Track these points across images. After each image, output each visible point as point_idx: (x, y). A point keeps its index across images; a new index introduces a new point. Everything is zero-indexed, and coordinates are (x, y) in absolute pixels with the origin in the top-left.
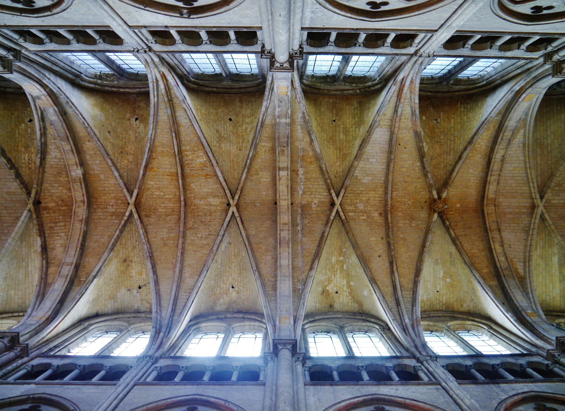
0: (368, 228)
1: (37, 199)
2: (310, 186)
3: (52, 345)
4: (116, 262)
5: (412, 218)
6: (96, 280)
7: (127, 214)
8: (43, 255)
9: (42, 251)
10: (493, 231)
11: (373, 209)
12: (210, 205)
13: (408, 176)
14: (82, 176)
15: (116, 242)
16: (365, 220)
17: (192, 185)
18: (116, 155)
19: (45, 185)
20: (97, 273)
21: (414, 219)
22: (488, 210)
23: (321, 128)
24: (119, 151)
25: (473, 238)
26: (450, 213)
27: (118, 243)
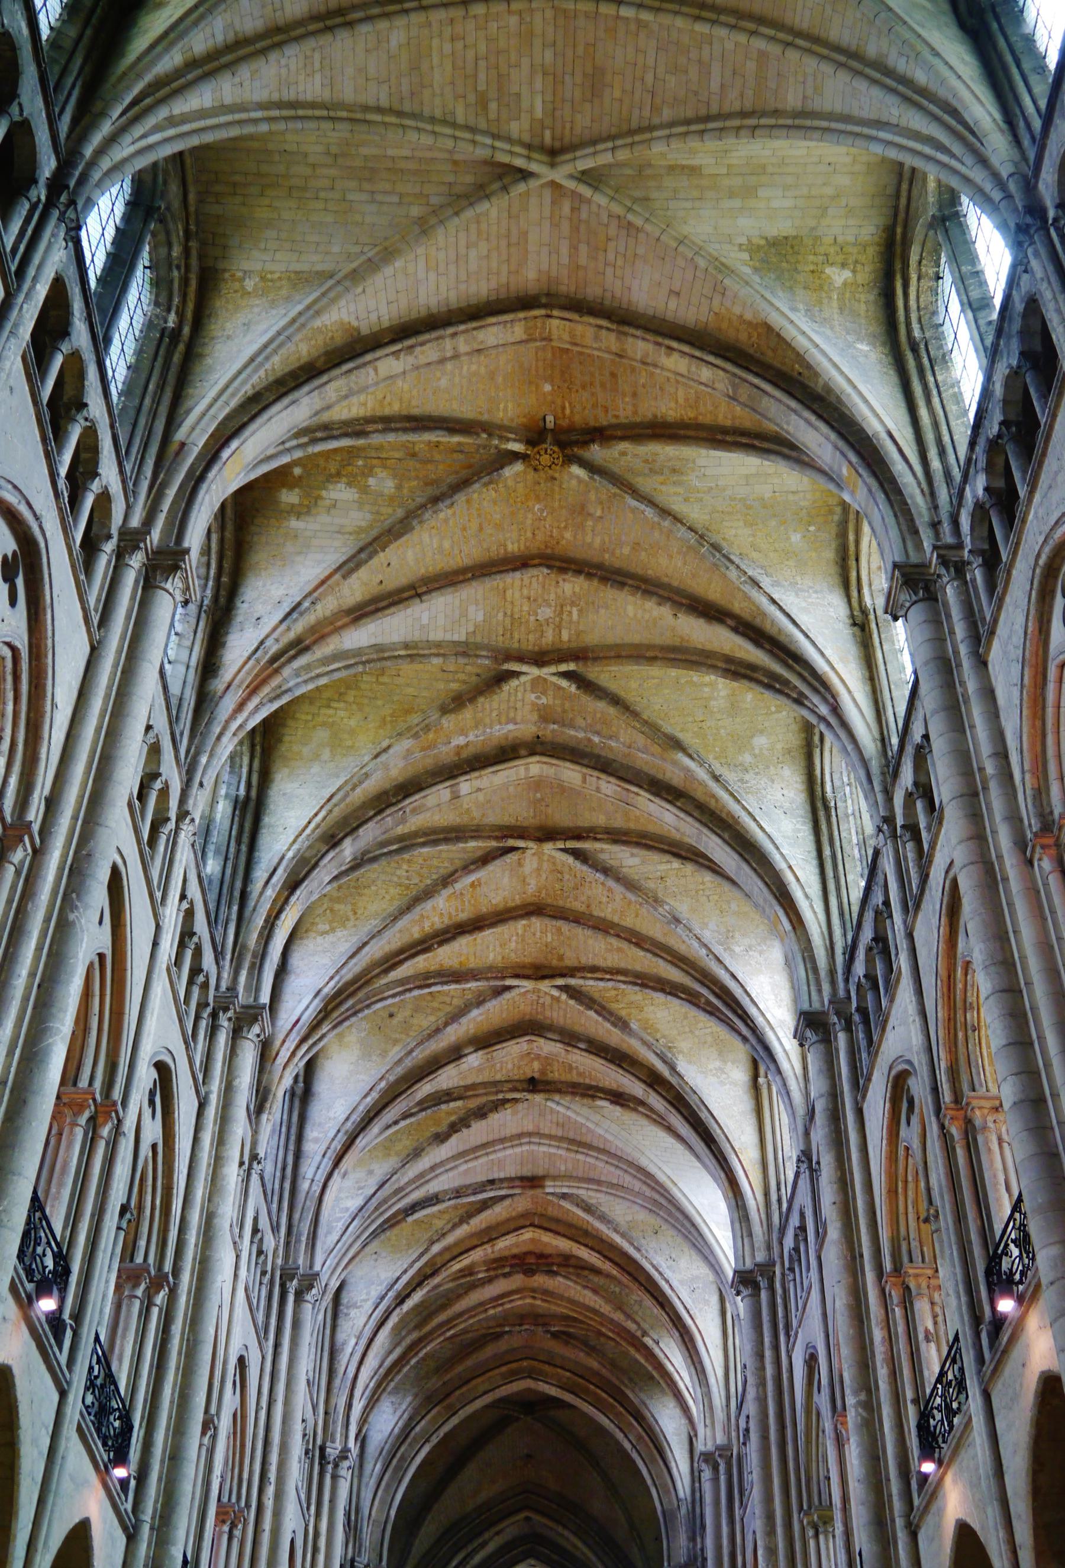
0: (602, 611)
1: (525, 1086)
2: (494, 714)
3: (774, 1197)
4: (652, 1008)
5: (581, 510)
6: (682, 1067)
7: (555, 993)
8: (628, 1107)
9: (622, 1105)
10: (623, 350)
11: (553, 589)
12: (538, 870)
13: (464, 529)
14: (480, 1053)
15: (611, 1013)
16: (580, 611)
17: (494, 902)
18: (435, 1004)
19: (498, 1077)
20: (665, 1062)
21: (583, 507)
22: (560, 339)
23: (348, 688)
24: (429, 998)
25: (642, 381)
26: (568, 412)
27: (614, 1006)
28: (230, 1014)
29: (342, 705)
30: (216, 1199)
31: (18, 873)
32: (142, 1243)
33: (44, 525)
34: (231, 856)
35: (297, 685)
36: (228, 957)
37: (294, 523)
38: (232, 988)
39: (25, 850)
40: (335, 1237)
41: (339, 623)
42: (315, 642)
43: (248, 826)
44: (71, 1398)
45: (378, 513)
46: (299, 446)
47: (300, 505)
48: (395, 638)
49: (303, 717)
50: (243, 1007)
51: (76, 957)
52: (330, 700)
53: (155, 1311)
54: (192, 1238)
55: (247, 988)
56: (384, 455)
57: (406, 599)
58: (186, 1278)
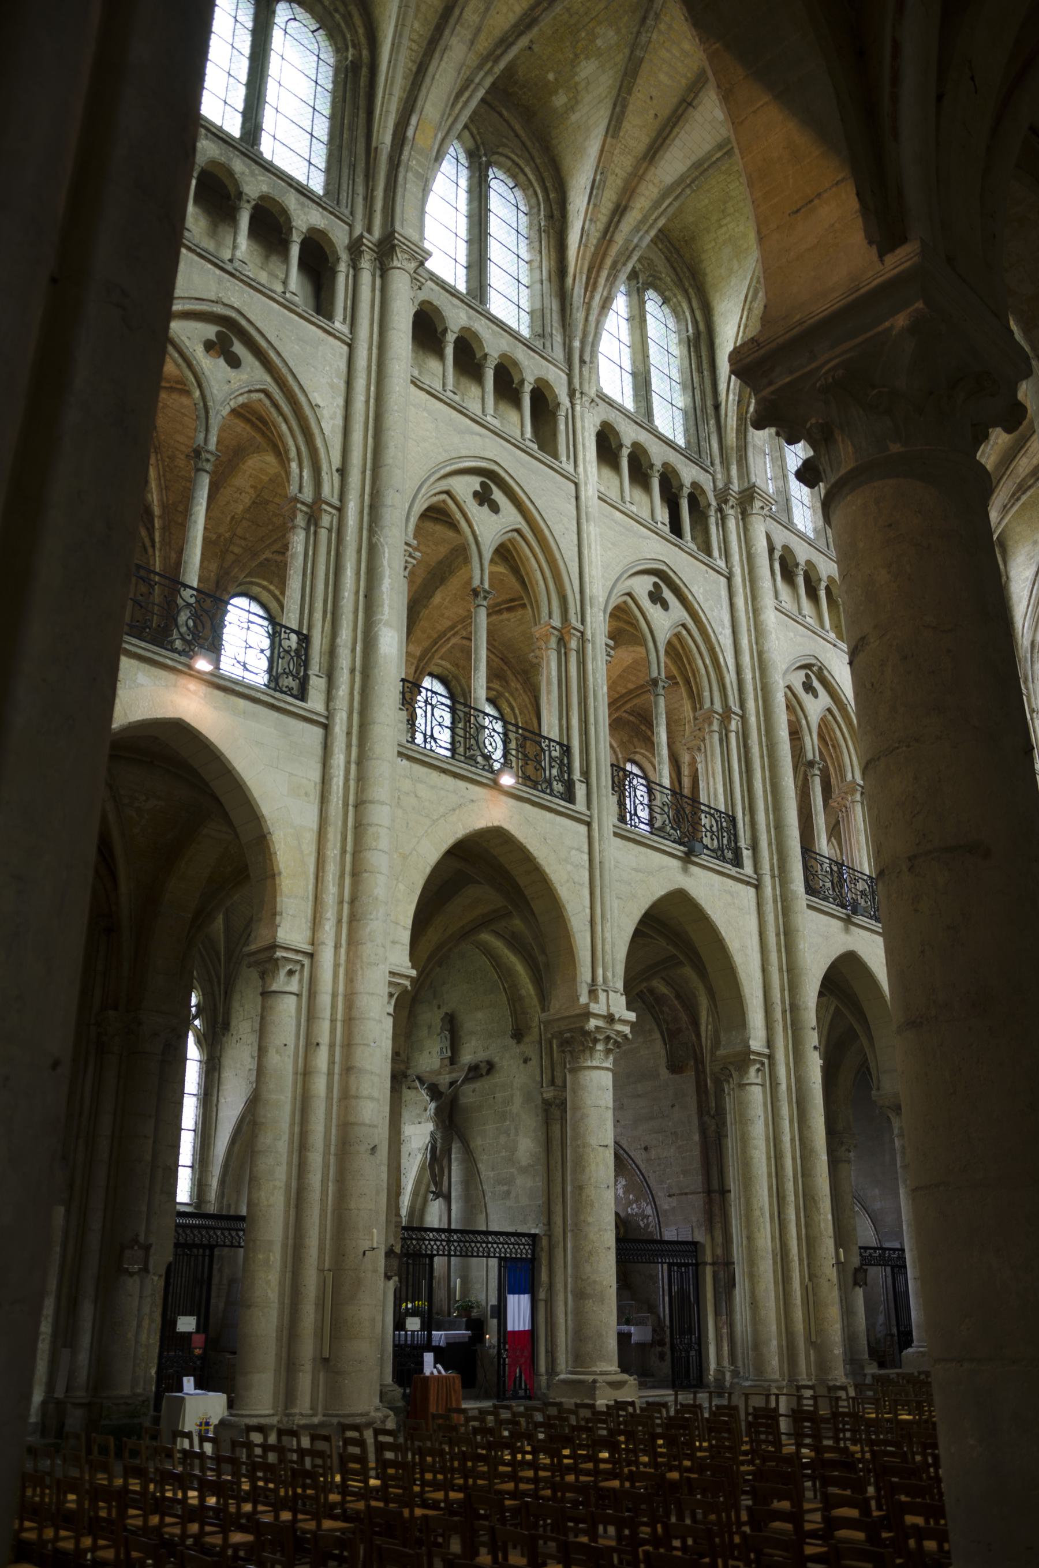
28: (732, 501)
29: (728, 219)
30: (760, 641)
31: (330, 531)
32: (706, 694)
33: (226, 301)
34: (696, 385)
35: (641, 239)
36: (717, 461)
37: (574, 118)
38: (729, 481)
39: (330, 513)
40: (1025, 603)
41: (641, 172)
42: (629, 200)
43: (704, 353)
44: (595, 826)
45: (616, 64)
46: (487, 74)
47: (570, 100)
48: (707, 147)
49: (710, 246)
50: (740, 493)
51: (382, 565)
52: (719, 220)
53: (733, 736)
54: (748, 676)
55: (740, 477)
56: (594, 14)
57: (682, 115)
58: (751, 705)
